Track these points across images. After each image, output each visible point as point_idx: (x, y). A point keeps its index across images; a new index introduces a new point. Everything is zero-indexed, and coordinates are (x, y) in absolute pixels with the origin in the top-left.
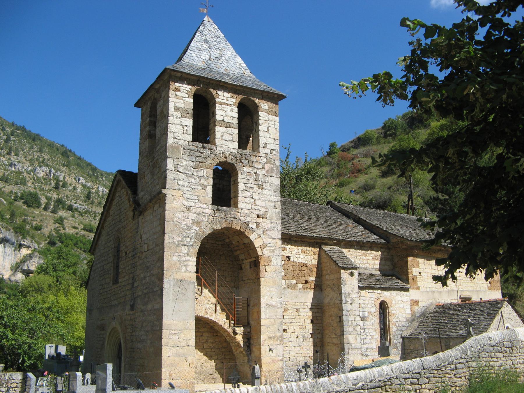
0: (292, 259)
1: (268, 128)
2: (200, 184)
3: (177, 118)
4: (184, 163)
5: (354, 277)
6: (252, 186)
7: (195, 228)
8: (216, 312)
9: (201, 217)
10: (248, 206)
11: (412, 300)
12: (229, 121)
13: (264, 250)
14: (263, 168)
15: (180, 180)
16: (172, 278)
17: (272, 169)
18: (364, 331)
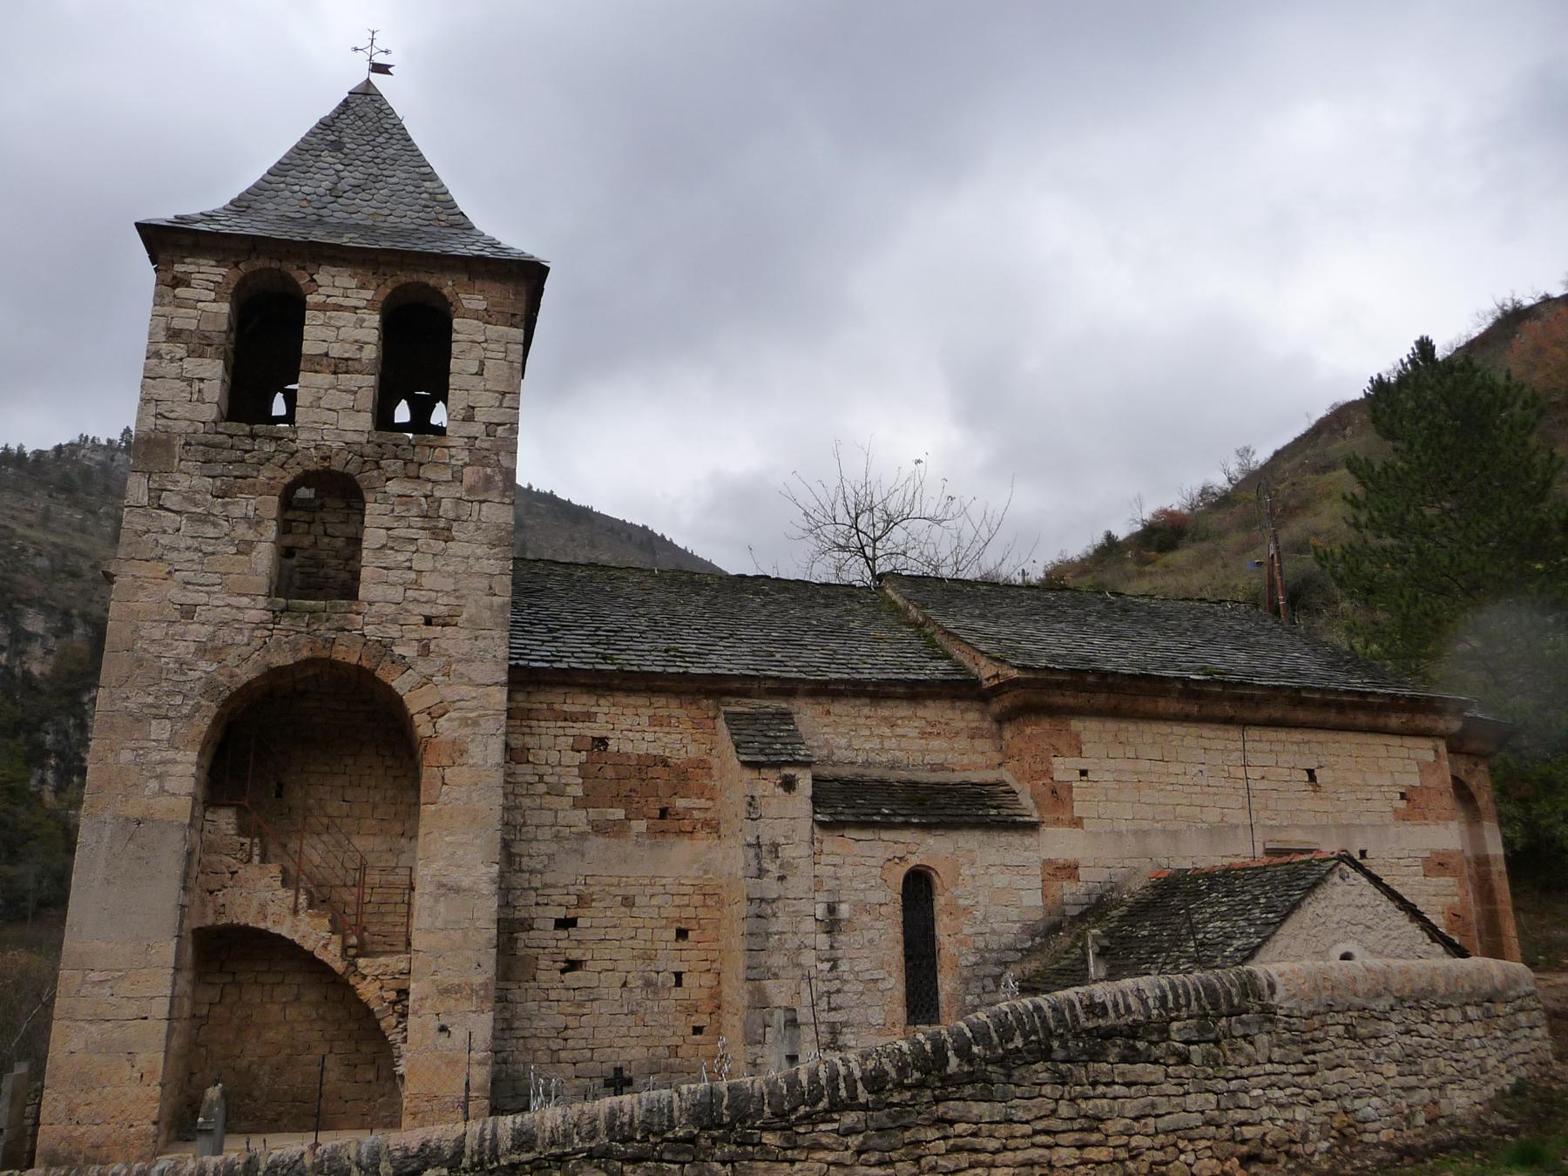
0: (613, 746)
1: (482, 364)
2: (232, 540)
3: (172, 360)
4: (184, 483)
5: (794, 794)
6: (412, 533)
7: (205, 666)
8: (295, 911)
9: (225, 634)
10: (396, 594)
11: (1047, 863)
12: (346, 355)
13: (441, 721)
14: (457, 478)
15: (165, 532)
16: (107, 816)
17: (488, 480)
18: (834, 968)
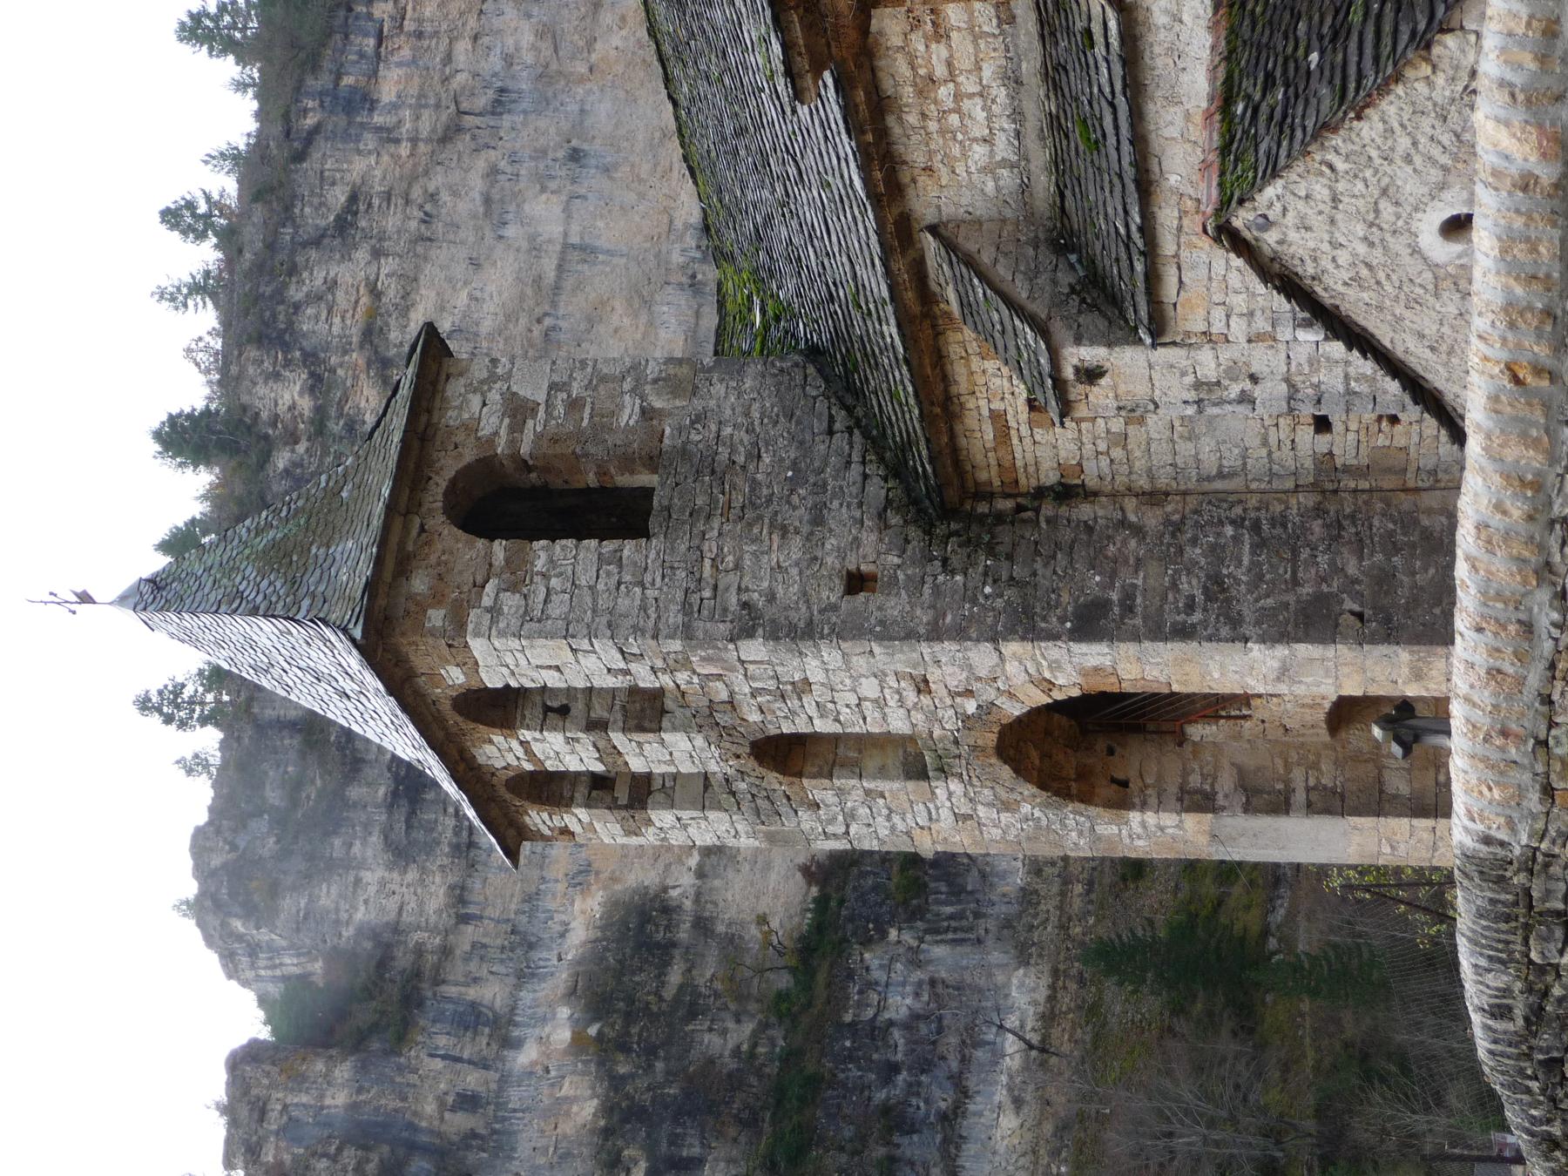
5: (1107, 365)
